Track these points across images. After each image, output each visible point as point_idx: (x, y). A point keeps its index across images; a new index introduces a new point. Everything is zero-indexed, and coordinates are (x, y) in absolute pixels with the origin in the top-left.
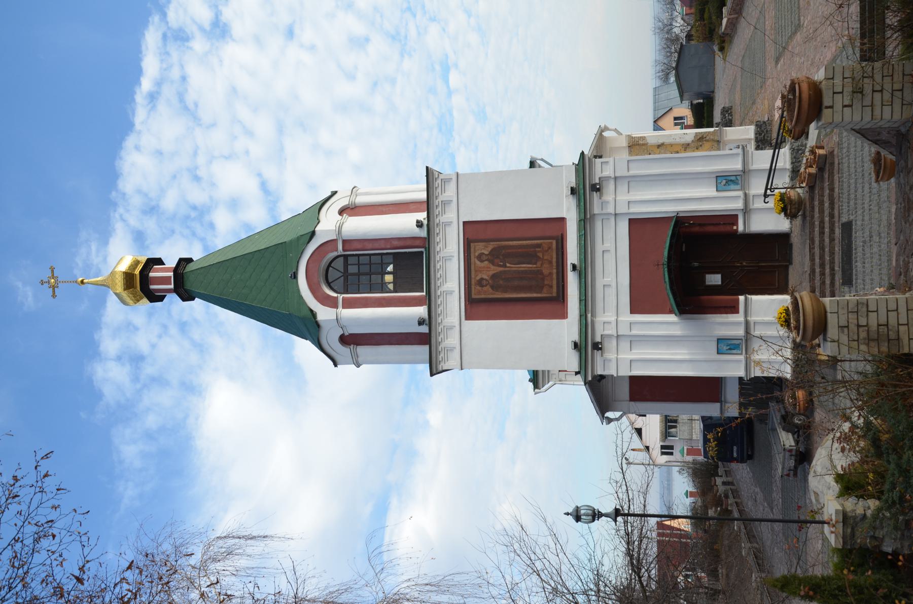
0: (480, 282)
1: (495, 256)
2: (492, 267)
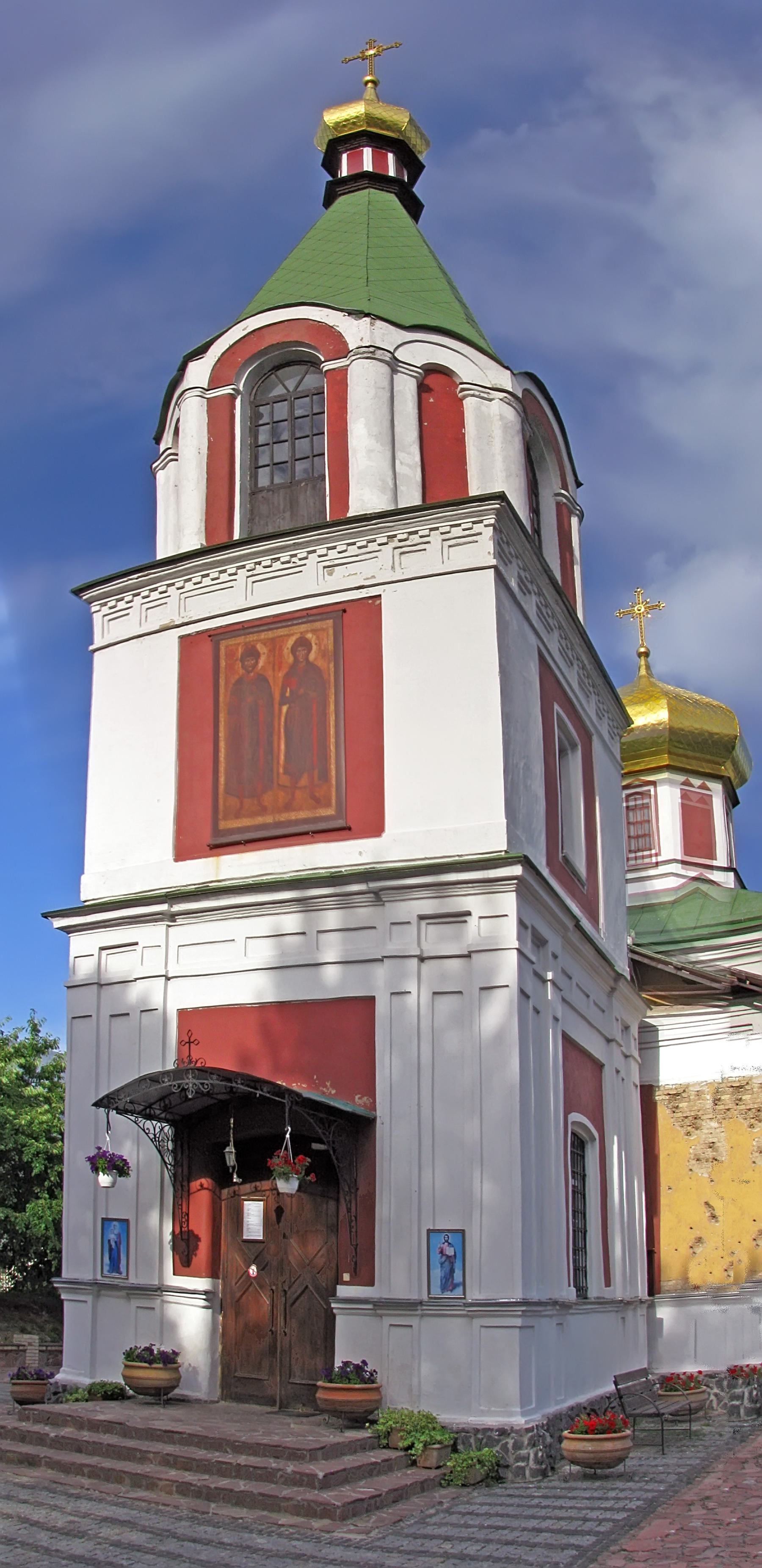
0: (252, 653)
2: (281, 675)
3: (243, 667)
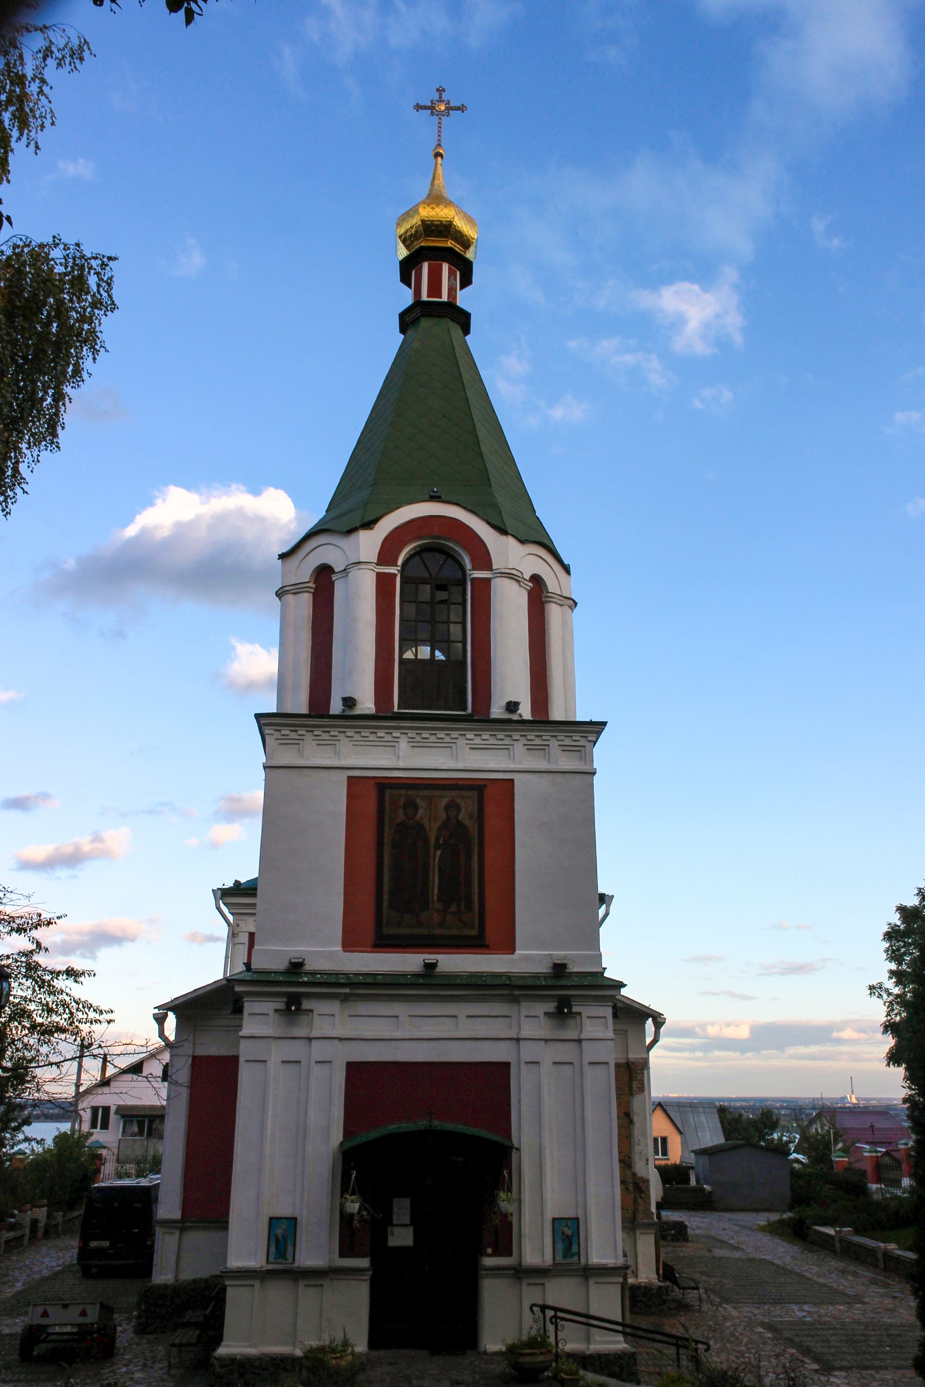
0: (411, 805)
2: (436, 826)
3: (405, 814)
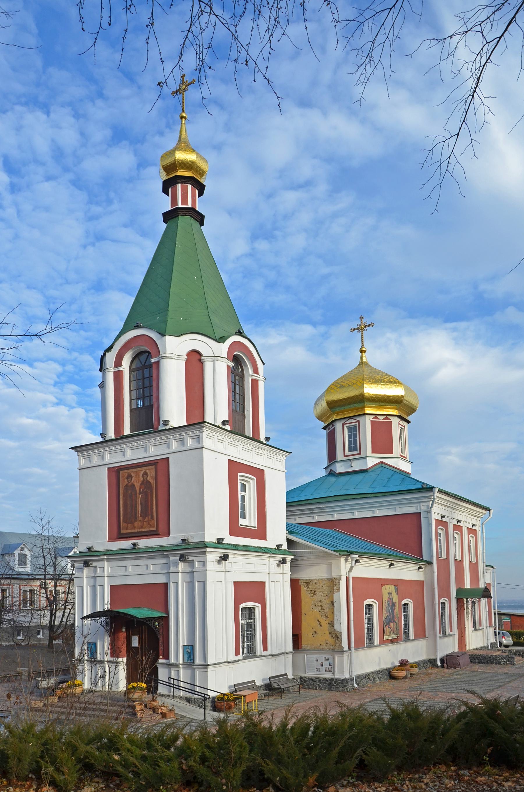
1: (146, 484)
2: (139, 484)
